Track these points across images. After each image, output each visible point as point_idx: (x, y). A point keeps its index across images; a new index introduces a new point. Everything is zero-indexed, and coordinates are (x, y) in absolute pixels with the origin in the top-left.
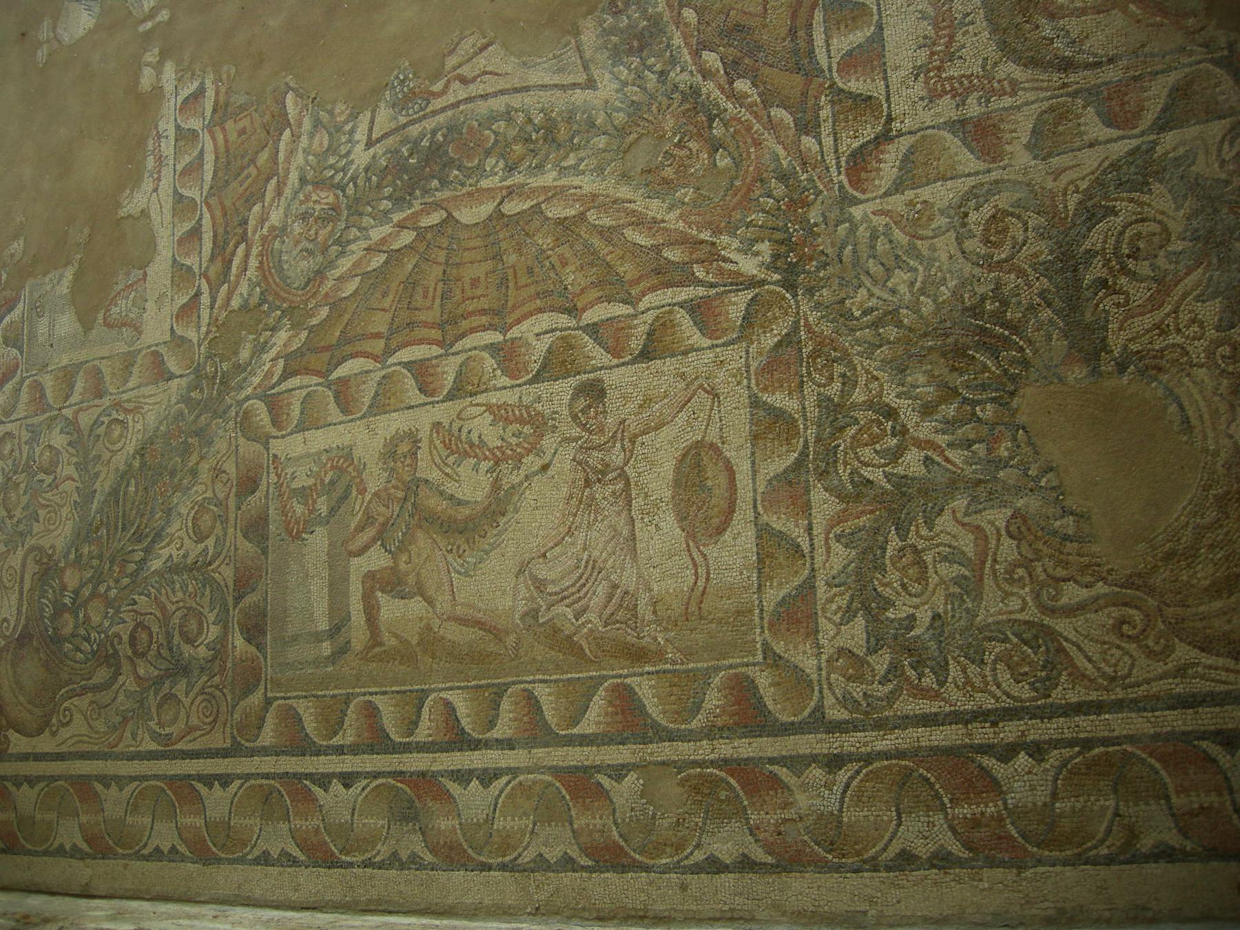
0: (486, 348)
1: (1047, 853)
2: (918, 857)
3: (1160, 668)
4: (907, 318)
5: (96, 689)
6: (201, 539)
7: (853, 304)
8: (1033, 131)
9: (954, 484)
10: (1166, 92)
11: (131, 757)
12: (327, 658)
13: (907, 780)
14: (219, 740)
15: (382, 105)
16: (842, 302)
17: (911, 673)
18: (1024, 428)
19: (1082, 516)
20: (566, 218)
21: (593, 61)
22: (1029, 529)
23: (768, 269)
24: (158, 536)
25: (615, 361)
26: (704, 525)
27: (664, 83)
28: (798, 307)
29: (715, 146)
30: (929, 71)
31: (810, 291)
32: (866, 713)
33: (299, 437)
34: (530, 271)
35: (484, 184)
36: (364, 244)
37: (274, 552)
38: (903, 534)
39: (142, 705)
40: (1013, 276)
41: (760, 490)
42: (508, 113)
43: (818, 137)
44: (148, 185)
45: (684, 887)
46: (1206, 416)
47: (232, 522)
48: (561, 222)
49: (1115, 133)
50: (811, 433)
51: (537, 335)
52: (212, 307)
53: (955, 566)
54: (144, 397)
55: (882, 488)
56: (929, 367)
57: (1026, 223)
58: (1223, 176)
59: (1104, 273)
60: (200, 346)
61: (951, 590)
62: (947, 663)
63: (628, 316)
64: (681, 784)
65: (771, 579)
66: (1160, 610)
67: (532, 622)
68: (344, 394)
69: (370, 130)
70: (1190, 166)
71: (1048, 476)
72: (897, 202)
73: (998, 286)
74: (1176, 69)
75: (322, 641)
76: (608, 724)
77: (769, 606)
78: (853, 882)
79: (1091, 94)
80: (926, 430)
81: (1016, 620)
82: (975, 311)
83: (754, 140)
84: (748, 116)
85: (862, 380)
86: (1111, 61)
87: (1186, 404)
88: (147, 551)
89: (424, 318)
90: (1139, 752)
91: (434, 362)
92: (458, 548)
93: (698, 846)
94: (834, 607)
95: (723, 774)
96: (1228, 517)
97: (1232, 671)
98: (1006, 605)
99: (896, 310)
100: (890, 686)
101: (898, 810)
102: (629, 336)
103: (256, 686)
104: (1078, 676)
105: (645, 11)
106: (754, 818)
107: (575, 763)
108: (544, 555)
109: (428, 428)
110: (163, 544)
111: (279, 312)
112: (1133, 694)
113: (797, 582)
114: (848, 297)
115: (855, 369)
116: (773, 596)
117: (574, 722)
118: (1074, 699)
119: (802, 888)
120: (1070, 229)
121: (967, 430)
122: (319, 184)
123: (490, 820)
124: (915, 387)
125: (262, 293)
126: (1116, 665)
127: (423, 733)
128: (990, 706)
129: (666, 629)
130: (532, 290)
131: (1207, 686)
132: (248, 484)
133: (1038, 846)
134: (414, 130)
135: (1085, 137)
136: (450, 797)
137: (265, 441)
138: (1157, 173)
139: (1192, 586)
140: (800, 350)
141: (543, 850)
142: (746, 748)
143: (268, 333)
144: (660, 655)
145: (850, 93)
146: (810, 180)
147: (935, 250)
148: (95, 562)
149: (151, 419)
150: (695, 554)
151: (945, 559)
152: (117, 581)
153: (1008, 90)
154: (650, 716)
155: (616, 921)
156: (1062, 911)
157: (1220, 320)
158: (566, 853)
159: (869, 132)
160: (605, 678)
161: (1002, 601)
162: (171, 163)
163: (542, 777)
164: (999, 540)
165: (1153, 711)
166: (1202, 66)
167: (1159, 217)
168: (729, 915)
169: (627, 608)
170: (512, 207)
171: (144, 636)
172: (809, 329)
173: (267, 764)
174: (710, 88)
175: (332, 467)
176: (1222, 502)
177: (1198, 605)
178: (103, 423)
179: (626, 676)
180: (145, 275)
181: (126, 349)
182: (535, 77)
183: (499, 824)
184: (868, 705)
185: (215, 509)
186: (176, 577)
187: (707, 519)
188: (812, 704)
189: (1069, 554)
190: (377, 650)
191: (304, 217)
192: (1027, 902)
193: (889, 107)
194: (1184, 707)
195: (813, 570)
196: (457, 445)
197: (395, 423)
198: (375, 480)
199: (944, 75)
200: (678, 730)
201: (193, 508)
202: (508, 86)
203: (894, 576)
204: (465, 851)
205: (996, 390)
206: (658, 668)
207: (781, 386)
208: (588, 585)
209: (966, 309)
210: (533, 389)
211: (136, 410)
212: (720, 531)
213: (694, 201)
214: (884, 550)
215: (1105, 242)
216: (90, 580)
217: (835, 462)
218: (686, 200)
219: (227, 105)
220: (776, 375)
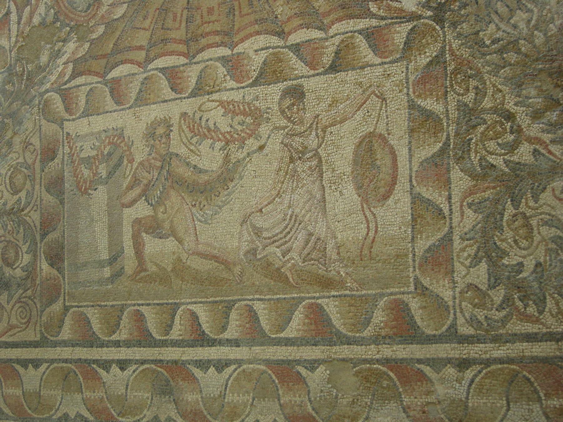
0: (219, 59)
7: (485, 35)
12: (108, 279)
14: (31, 335)
17: (519, 304)
23: (423, 7)
25: (312, 72)
26: (374, 193)
28: (445, 36)
31: (454, 25)
32: (487, 331)
33: (85, 121)
37: (68, 202)
38: (516, 203)
41: (415, 169)
47: (38, 181)
50: (452, 129)
51: (256, 51)
52: (19, 23)
53: (553, 229)
55: (502, 171)
56: (539, 84)
60: (11, 51)
61: (550, 246)
62: (545, 298)
63: (322, 39)
64: (357, 374)
65: (421, 233)
67: (252, 257)
68: (116, 90)
75: (104, 267)
76: (305, 331)
77: (419, 252)
80: (534, 130)
85: (490, 92)
89: (174, 36)
91: (181, 68)
92: (200, 203)
94: (466, 254)
95: (385, 369)
99: (517, 41)
100: (504, 313)
102: (322, 54)
103: (57, 297)
106: (406, 400)
107: (282, 358)
108: (261, 210)
109: (177, 117)
111: (68, 29)
113: (439, 235)
114: (481, 30)
115: (485, 84)
116: (423, 244)
117: (282, 329)
123: (223, 396)
124: (528, 98)
125: (55, 14)
127: (175, 334)
129: (346, 266)
130: (252, 18)
132: (49, 153)
136: (194, 379)
137: (61, 122)
140: (445, 68)
142: (401, 351)
143: (61, 44)
144: (342, 284)
150: (368, 213)
151: (546, 223)
154: (334, 327)
160: (303, 299)
163: (259, 366)
169: (319, 250)
172: (452, 53)
173: (66, 353)
175: (109, 143)
179: (318, 298)
184: (488, 325)
185: (26, 171)
187: (376, 188)
188: (449, 322)
190: (143, 274)
195: (451, 227)
196: (199, 130)
197: (153, 113)
198: (140, 153)
200: (354, 337)
201: (9, 170)
203: (509, 234)
204: (205, 417)
206: (340, 293)
207: (431, 94)
208: (292, 233)
210: (252, 90)
212: (386, 197)
214: (502, 215)
217: (469, 150)
220: (428, 86)
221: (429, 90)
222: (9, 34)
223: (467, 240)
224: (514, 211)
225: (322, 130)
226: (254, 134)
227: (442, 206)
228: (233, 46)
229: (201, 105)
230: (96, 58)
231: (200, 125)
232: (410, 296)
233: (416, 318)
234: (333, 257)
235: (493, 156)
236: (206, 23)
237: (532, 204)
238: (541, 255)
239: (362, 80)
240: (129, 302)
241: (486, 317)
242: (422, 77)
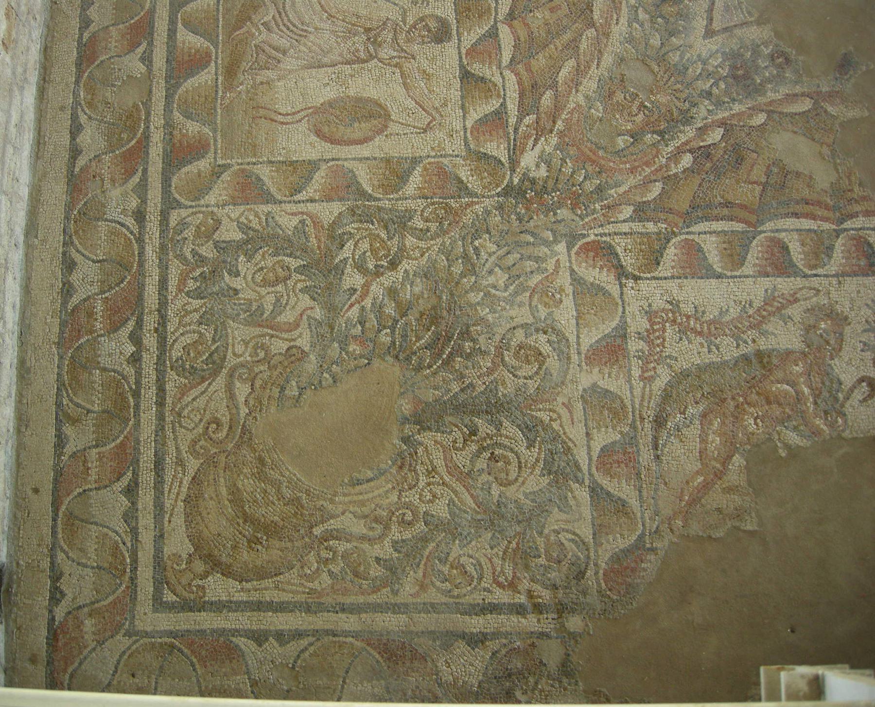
2: (70, 274)
3: (184, 448)
4: (468, 281)
8: (607, 391)
9: (332, 309)
13: (123, 267)
16: (488, 232)
18: (369, 364)
19: (297, 401)
20: (592, 11)
22: (292, 363)
25: (464, 51)
26: (324, 120)
27: (700, 95)
28: (488, 197)
29: (636, 136)
30: (673, 313)
31: (500, 207)
32: (172, 240)
40: (489, 364)
41: (346, 164)
43: (631, 219)
45: (62, 109)
46: (361, 497)
49: (595, 455)
50: (387, 204)
53: (271, 308)
56: (426, 296)
57: (531, 378)
58: (546, 531)
59: (481, 433)
62: (202, 298)
63: (500, 62)
64: (135, 106)
65: (277, 171)
66: (224, 452)
70: (559, 508)
71: (330, 379)
72: (564, 280)
73: (484, 353)
74: (641, 506)
78: (58, 228)
79: (631, 440)
81: (227, 349)
82: (466, 334)
83: (636, 168)
85: (422, 244)
86: (657, 457)
87: (372, 484)
90: (128, 429)
93: (90, 118)
94: (251, 218)
95: (139, 135)
96: (284, 505)
97: (177, 497)
98: (239, 343)
99: (475, 274)
100: (189, 256)
101: (104, 260)
104: (183, 391)
105: (770, 82)
106: (107, 158)
113: (273, 190)
115: (432, 239)
116: (265, 173)
117: (187, 24)
120: (522, 412)
121: (372, 322)
126: (188, 417)
128: (169, 327)
129: (248, 92)
131: (168, 478)
133: (72, 357)
138: (557, 482)
139: (239, 475)
142: (156, 152)
145: (665, 248)
146: (594, 211)
147: (519, 306)
150: (303, 113)
151: (278, 300)
153: (646, 375)
154: (185, 81)
155: (43, 60)
156: (28, 371)
157: (433, 516)
158: (93, 22)
159: (628, 261)
160: (216, 47)
164: (287, 340)
165: (155, 441)
166: (640, 526)
167: (521, 480)
168: (42, 141)
169: (267, 62)
172: (468, 205)
174: (689, 133)
176: (295, 502)
177: (225, 479)
179: (216, 63)
184: (178, 241)
188: (183, 200)
192: (35, 348)
193: (648, 279)
194: (155, 462)
195: (281, 202)
199: (667, 324)
203: (270, 262)
205: (401, 346)
206: (220, 86)
207: (426, 182)
208: (288, 33)
212: (319, 133)
213: (591, 117)
214: (290, 256)
215: (507, 437)
217: (361, 221)
218: (593, 111)
221: (431, 179)
224: (293, 267)
225: (397, 63)
227: (304, 192)
232: (212, 160)
234: (258, 77)
235: (352, 247)
237: (300, 286)
238: (247, 294)
239: (449, 106)
241: (186, 239)
242: (446, 172)
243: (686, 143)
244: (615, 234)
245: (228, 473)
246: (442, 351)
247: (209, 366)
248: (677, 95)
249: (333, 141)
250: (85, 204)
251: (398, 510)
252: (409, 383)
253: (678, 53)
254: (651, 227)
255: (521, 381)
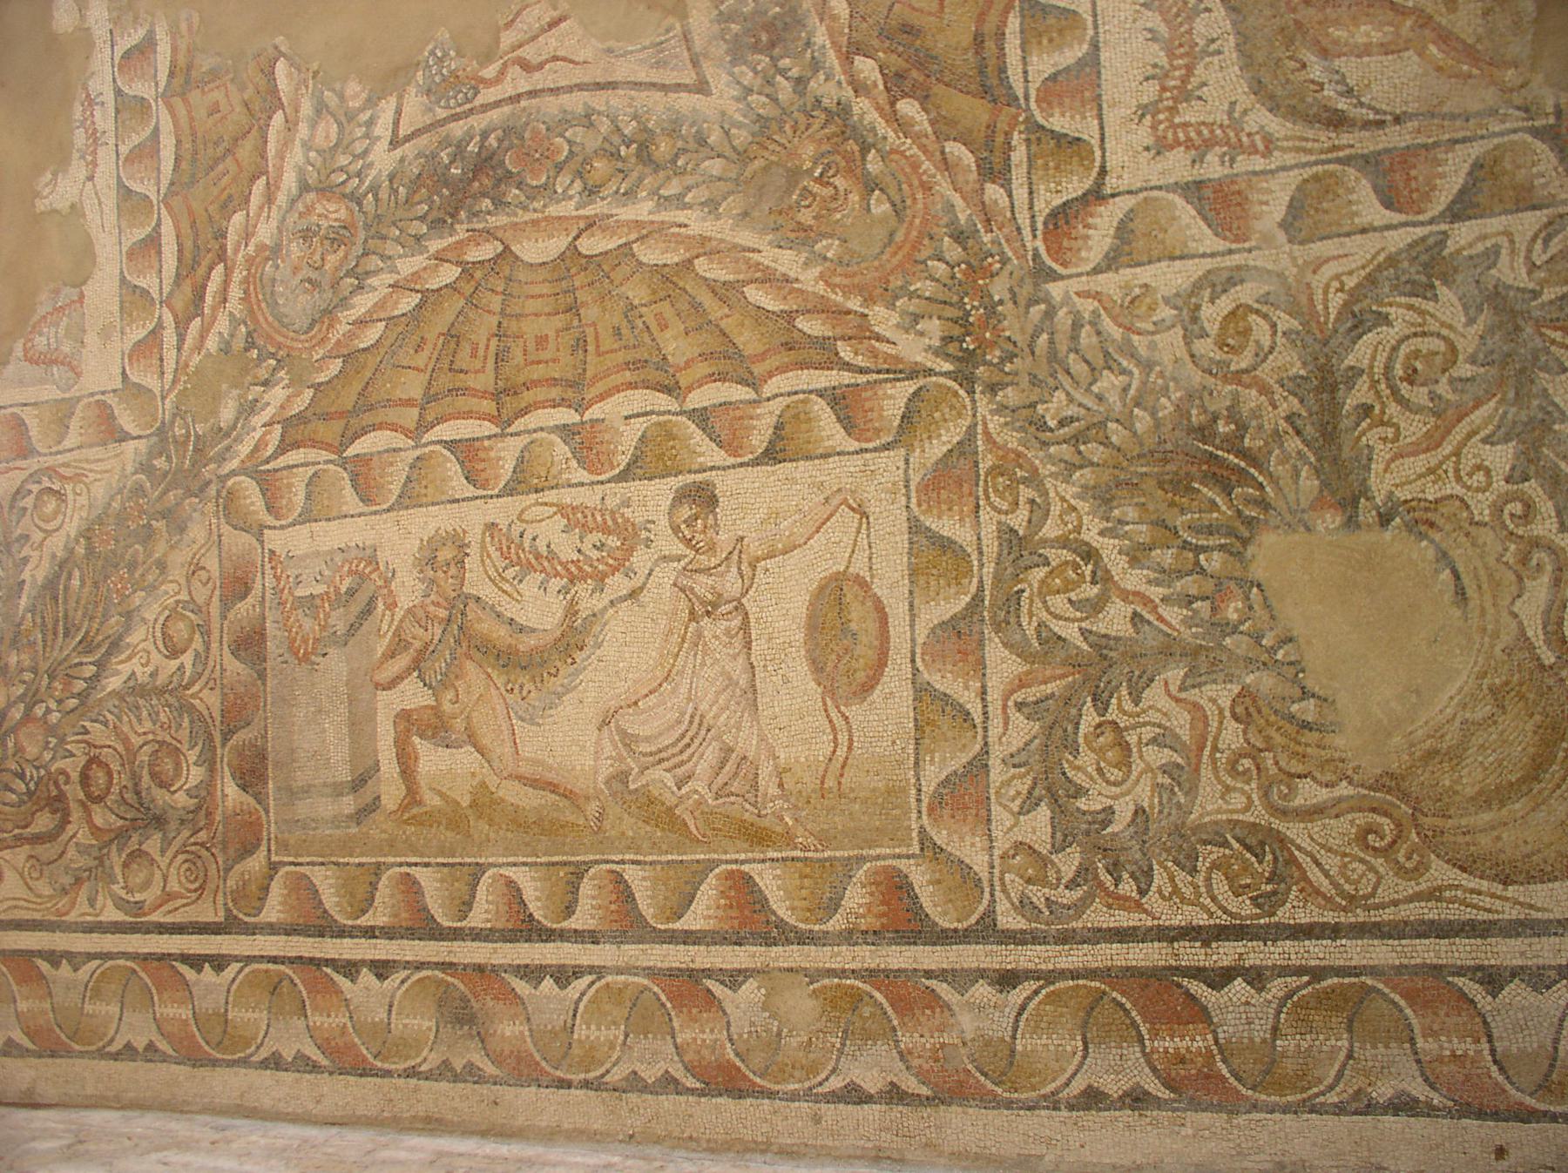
1: (1264, 1097)
3: (1411, 888)
4: (1117, 434)
5: (37, 839)
6: (174, 653)
7: (1047, 410)
8: (1290, 206)
9: (1169, 650)
10: (1466, 167)
11: (90, 929)
14: (208, 912)
15: (412, 90)
16: (1033, 405)
18: (1259, 586)
21: (705, 56)
22: (1259, 712)
24: (115, 645)
25: (731, 461)
27: (802, 94)
28: (974, 409)
29: (870, 186)
31: (992, 389)
33: (304, 530)
34: (617, 332)
35: (553, 210)
36: (390, 279)
38: (1102, 706)
39: (102, 864)
41: (920, 640)
42: (588, 116)
44: (78, 170)
45: (817, 1119)
48: (657, 269)
49: (1397, 218)
50: (989, 569)
54: (87, 461)
57: (1274, 326)
58: (1531, 286)
59: (1369, 399)
60: (163, 398)
61: (1159, 780)
65: (932, 752)
69: (396, 123)
70: (1489, 268)
72: (1109, 283)
75: (342, 794)
77: (929, 787)
79: (1367, 162)
80: (1134, 579)
82: (1204, 432)
84: (915, 150)
85: (1056, 509)
86: (1397, 120)
88: (100, 664)
91: (486, 443)
93: (834, 1071)
94: (1012, 793)
95: (868, 988)
97: (1499, 897)
98: (1227, 802)
100: (1078, 893)
106: (905, 1041)
107: (677, 965)
109: (479, 530)
110: (123, 657)
112: (1375, 917)
113: (965, 758)
116: (932, 775)
118: (1303, 918)
119: (964, 1125)
121: (1189, 584)
122: (325, 191)
125: (249, 334)
127: (478, 918)
130: (621, 357)
131: (1470, 914)
132: (237, 586)
133: (1254, 1088)
134: (458, 129)
135: (1357, 220)
136: (514, 997)
137: (259, 532)
140: (976, 464)
141: (639, 1067)
142: (898, 957)
144: (788, 839)
148: (28, 676)
149: (100, 492)
150: (834, 714)
152: (60, 702)
153: (1261, 146)
154: (774, 913)
157: (1513, 469)
159: (1075, 187)
161: (1222, 798)
162: (112, 141)
163: (636, 979)
164: (1221, 723)
167: (1445, 332)
170: (591, 245)
171: (99, 776)
174: (864, 110)
175: (350, 572)
178: (30, 492)
179: (743, 862)
180: (82, 296)
181: (59, 395)
182: (623, 70)
183: (581, 1032)
186: (141, 702)
188: (981, 909)
189: (1307, 745)
190: (415, 811)
191: (306, 235)
192: (1239, 1154)
193: (1103, 156)
196: (522, 558)
198: (408, 590)
199: (1177, 120)
200: (811, 931)
202: (586, 80)
203: (1087, 758)
204: (538, 1064)
207: (950, 509)
209: (1191, 430)
210: (620, 488)
211: (77, 478)
212: (867, 688)
215: (1373, 358)
216: (21, 698)
218: (829, 255)
219: (189, 67)
222: (161, 366)
223: (1014, 766)
226: (620, 564)
228: (580, 408)
229: (522, 512)
230: (327, 417)
231: (520, 546)
233: (922, 900)
236: (533, 363)
237: (1128, 706)
238: (1144, 794)
240: (391, 859)
243: (879, 108)
244: (1031, 208)
245: (1452, 812)
246: (1235, 469)
247: (1266, 853)
248: (803, 128)
249: (882, 662)
250: (985, 1075)
251: (1505, 527)
252: (1288, 517)
253: (733, 131)
254: (1019, 155)
255: (1279, 339)
